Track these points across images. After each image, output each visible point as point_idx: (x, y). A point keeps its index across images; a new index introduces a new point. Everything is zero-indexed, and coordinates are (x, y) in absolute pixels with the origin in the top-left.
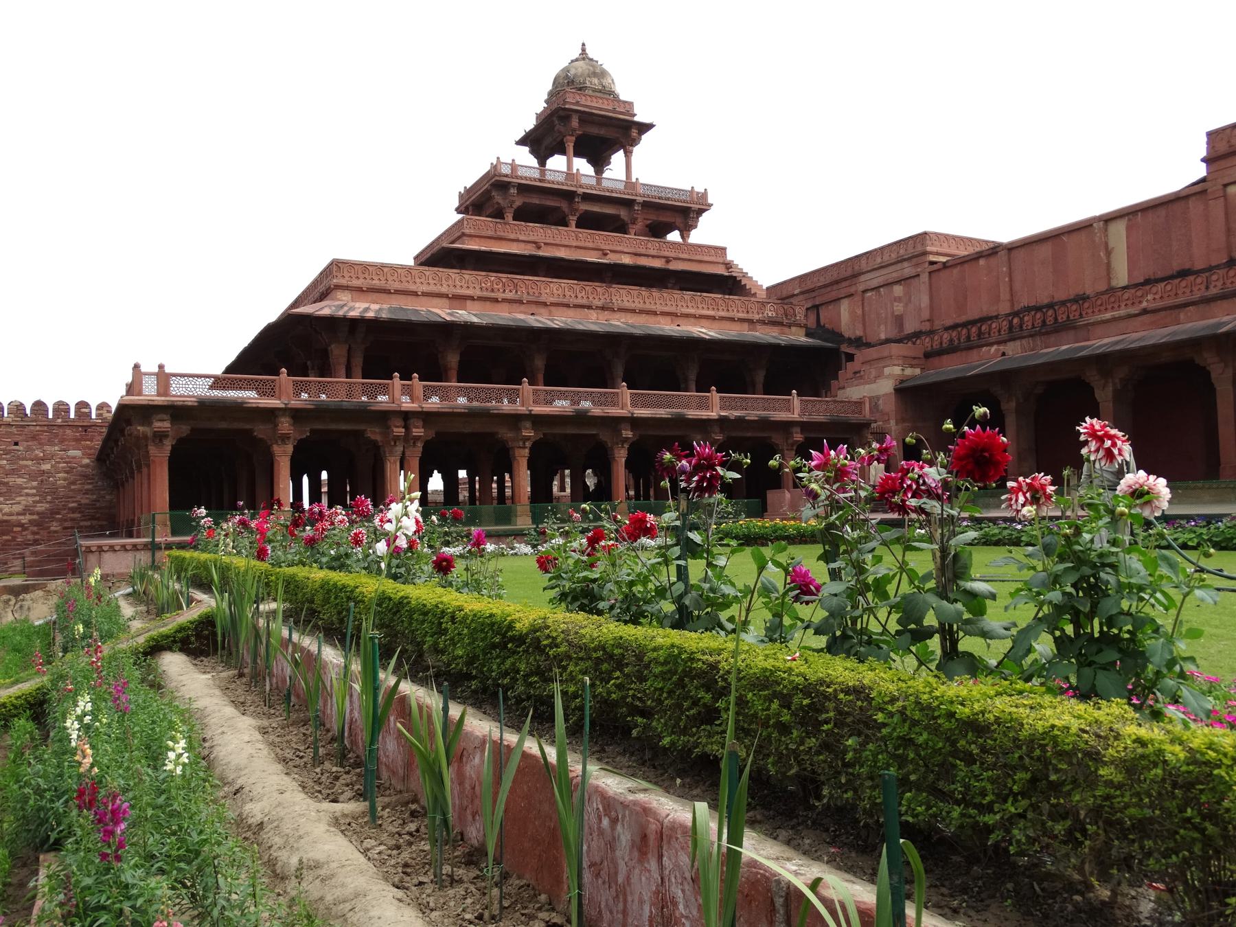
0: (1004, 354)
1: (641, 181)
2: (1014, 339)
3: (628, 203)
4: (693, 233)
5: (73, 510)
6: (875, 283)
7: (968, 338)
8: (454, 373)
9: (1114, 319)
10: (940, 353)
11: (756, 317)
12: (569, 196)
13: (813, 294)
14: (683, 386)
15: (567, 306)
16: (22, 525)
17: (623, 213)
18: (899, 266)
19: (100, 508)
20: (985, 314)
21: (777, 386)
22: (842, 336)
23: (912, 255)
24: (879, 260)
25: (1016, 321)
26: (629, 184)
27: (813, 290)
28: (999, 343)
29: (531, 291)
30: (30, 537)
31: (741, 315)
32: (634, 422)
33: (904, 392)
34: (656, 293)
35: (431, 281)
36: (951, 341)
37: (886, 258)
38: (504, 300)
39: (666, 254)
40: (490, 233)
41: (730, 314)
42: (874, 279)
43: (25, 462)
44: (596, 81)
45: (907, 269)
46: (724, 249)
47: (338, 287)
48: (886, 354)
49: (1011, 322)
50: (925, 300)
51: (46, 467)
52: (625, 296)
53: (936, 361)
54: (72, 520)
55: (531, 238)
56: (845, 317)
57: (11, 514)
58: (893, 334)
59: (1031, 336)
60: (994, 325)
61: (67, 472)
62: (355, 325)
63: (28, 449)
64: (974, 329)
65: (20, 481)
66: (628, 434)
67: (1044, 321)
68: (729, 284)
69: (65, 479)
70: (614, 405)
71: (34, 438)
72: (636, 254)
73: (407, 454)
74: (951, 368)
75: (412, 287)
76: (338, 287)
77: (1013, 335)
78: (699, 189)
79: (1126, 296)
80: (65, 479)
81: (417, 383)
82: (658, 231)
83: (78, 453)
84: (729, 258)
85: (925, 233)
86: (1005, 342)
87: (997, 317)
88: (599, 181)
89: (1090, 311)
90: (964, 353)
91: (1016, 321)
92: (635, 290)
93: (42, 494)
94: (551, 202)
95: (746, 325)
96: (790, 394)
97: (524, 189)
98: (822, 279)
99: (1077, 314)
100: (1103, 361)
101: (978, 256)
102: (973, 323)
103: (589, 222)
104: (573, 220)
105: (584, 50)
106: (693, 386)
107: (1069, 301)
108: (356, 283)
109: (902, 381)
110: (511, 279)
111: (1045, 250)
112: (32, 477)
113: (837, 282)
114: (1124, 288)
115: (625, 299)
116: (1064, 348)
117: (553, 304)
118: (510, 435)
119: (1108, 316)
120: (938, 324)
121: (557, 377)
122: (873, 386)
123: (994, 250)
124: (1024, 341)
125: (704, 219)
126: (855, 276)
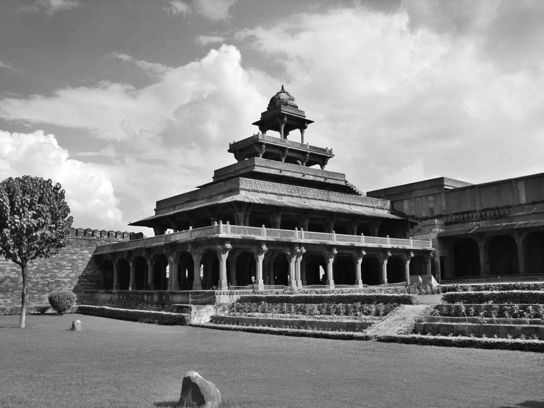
1: (309, 144)
2: (482, 220)
3: (304, 153)
4: (326, 166)
6: (421, 195)
7: (463, 218)
8: (279, 226)
9: (522, 215)
10: (451, 223)
11: (376, 206)
12: (283, 149)
15: (316, 200)
16: (64, 283)
19: (95, 277)
21: (382, 234)
22: (404, 214)
24: (422, 186)
25: (483, 213)
26: (302, 145)
28: (476, 221)
30: (68, 288)
32: (366, 249)
36: (456, 219)
38: (296, 197)
39: (325, 176)
40: (264, 165)
43: (67, 255)
44: (291, 102)
47: (242, 189)
48: (433, 223)
50: (444, 204)
51: (75, 257)
52: (334, 196)
53: (449, 226)
54: (84, 281)
56: (406, 207)
57: (60, 278)
59: (490, 219)
60: (474, 214)
61: (82, 260)
62: (250, 205)
63: (68, 249)
64: (466, 216)
65: (65, 263)
68: (347, 190)
69: (81, 263)
70: (360, 242)
71: (71, 244)
72: (315, 176)
74: (457, 230)
75: (266, 190)
76: (242, 189)
77: (482, 218)
78: (329, 149)
80: (81, 263)
81: (229, 226)
84: (347, 179)
86: (478, 221)
91: (483, 213)
92: (337, 194)
93: (73, 270)
94: (276, 151)
97: (268, 145)
100: (520, 230)
102: (466, 213)
103: (290, 160)
105: (283, 88)
106: (356, 233)
108: (247, 188)
109: (439, 234)
113: (403, 193)
114: (526, 204)
116: (504, 224)
117: (311, 199)
118: (327, 253)
119: (520, 214)
120: (448, 213)
121: (311, 228)
122: (428, 235)
125: (330, 161)
126: (411, 191)
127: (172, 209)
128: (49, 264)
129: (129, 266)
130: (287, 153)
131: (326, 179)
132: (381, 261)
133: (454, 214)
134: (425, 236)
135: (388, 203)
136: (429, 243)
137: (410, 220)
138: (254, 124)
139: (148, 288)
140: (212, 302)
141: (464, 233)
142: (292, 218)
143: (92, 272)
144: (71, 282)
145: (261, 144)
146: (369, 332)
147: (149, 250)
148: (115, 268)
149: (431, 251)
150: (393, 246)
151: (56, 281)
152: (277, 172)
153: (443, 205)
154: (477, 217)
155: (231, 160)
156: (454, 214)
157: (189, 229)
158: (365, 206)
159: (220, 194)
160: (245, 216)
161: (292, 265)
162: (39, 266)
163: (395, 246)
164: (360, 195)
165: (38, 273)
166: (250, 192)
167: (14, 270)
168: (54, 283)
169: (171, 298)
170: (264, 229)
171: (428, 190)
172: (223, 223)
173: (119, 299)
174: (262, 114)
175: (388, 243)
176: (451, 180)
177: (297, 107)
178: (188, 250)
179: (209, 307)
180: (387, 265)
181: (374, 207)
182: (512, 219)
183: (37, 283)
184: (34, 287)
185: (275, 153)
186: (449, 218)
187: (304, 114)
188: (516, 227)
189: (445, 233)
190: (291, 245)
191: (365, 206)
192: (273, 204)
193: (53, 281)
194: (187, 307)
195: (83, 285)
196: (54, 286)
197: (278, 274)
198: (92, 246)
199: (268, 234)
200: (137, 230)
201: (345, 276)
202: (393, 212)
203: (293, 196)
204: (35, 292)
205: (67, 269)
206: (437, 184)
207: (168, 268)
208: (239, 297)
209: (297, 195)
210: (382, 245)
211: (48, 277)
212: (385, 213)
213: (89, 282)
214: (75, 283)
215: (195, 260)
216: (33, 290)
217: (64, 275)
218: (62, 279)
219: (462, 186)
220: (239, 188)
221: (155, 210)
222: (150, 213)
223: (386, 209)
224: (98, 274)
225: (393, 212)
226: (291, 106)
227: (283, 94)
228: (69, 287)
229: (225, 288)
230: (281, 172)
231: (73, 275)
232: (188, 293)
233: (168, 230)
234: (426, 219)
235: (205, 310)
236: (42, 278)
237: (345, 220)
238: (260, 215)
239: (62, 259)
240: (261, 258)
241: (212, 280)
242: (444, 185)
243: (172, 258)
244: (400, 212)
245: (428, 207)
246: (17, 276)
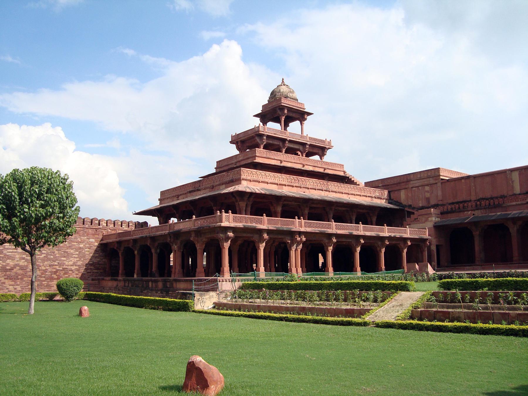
0: (474, 215)
1: (309, 136)
3: (304, 145)
4: (325, 156)
6: (417, 185)
7: (459, 208)
8: (279, 215)
9: (517, 205)
10: (447, 213)
11: (373, 196)
12: (284, 140)
15: (315, 189)
16: (72, 270)
18: (428, 179)
21: (380, 223)
24: (419, 176)
26: (302, 136)
28: (472, 210)
30: (75, 276)
31: (369, 195)
32: (364, 237)
34: (342, 185)
36: (452, 208)
37: (422, 175)
38: (296, 186)
40: (265, 156)
41: (365, 194)
44: (291, 95)
45: (432, 181)
47: (243, 179)
50: (440, 193)
51: (82, 246)
52: (333, 186)
54: (91, 269)
56: (403, 196)
58: (425, 204)
59: (485, 209)
60: (469, 204)
62: (251, 194)
63: (76, 238)
64: (461, 205)
65: (72, 251)
67: (489, 204)
68: (345, 180)
70: (358, 230)
71: (78, 233)
74: (453, 219)
75: (267, 180)
76: (243, 179)
77: (477, 208)
78: (328, 140)
79: (520, 197)
81: (231, 215)
83: (93, 240)
84: (345, 170)
85: (439, 168)
86: (474, 210)
87: (471, 201)
91: (478, 203)
93: (80, 258)
94: (276, 142)
97: (269, 137)
100: (514, 220)
101: (462, 178)
102: (461, 202)
103: (290, 151)
106: (354, 221)
108: (249, 178)
109: (435, 223)
112: (76, 250)
113: (400, 183)
114: (520, 194)
116: (499, 213)
117: (311, 189)
119: (514, 203)
120: (445, 202)
121: (311, 217)
122: (424, 224)
123: (468, 177)
125: (328, 152)
126: (408, 181)
127: (176, 198)
128: (56, 252)
129: (134, 255)
130: (287, 144)
131: (325, 169)
132: (378, 249)
135: (386, 192)
136: (425, 232)
137: (407, 209)
139: (152, 275)
140: (214, 289)
141: (460, 222)
142: (292, 207)
144: (78, 270)
145: (261, 136)
146: (367, 318)
147: (153, 239)
148: (120, 256)
150: (390, 234)
151: (64, 269)
152: (278, 163)
155: (233, 151)
156: (450, 204)
157: (192, 218)
159: (222, 184)
160: (246, 205)
161: (293, 253)
162: (47, 254)
163: (393, 235)
164: (359, 185)
165: (47, 261)
166: (252, 182)
167: (24, 258)
168: (61, 270)
169: (174, 285)
170: (265, 218)
171: (424, 180)
172: (226, 212)
173: (125, 286)
174: (263, 106)
175: (386, 231)
176: (447, 170)
177: (297, 100)
178: (192, 239)
179: (212, 293)
181: (372, 197)
182: (506, 208)
183: (46, 271)
184: (42, 274)
185: (275, 144)
187: (304, 106)
188: (509, 216)
189: (441, 222)
190: (292, 234)
192: (273, 193)
193: (61, 268)
194: (191, 294)
195: (90, 272)
197: (279, 261)
199: (269, 222)
200: (142, 219)
201: (343, 263)
202: (390, 201)
203: (293, 186)
204: (44, 279)
205: (75, 257)
206: (434, 174)
207: (172, 256)
208: (241, 283)
209: (297, 185)
210: (379, 233)
211: (56, 265)
212: (382, 203)
214: (82, 270)
215: (198, 248)
216: (42, 277)
217: (71, 263)
218: (70, 267)
219: (458, 176)
220: (240, 178)
221: (159, 200)
222: (154, 203)
223: (383, 199)
225: (390, 201)
226: (291, 98)
227: (283, 87)
228: (77, 274)
229: (227, 276)
230: (281, 162)
231: (80, 263)
232: (191, 281)
233: (172, 219)
234: (422, 208)
235: (208, 296)
236: (50, 266)
237: (344, 209)
238: (262, 204)
239: (70, 247)
240: (262, 247)
241: (215, 268)
242: (440, 175)
243: (176, 247)
244: (397, 202)
245: (425, 196)
246: (26, 264)
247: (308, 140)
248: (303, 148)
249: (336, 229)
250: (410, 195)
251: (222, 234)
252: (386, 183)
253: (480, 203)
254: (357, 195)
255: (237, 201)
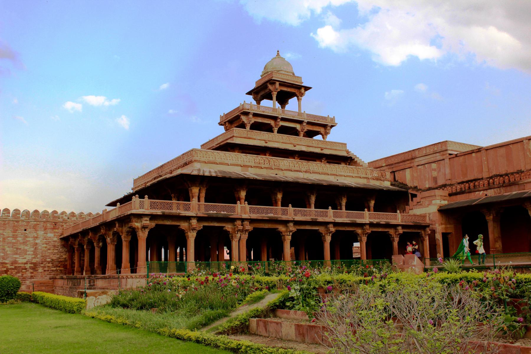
0: (486, 195)
2: (491, 189)
4: (328, 136)
5: (49, 262)
6: (423, 162)
7: (469, 187)
10: (456, 194)
13: (392, 166)
14: (339, 208)
16: (26, 269)
17: (298, 127)
20: (476, 177)
22: (406, 185)
23: (440, 151)
24: (424, 152)
26: (299, 114)
27: (392, 165)
28: (483, 190)
29: (276, 164)
33: (443, 211)
35: (234, 159)
36: (461, 189)
37: (428, 151)
40: (245, 136)
42: (423, 160)
43: (27, 239)
45: (438, 157)
46: (346, 144)
47: (195, 161)
48: (433, 194)
49: (489, 181)
50: (448, 171)
53: (454, 197)
54: (49, 267)
55: (263, 138)
56: (408, 178)
57: (22, 263)
58: (432, 185)
60: (481, 182)
61: (46, 244)
64: (472, 184)
66: (332, 229)
70: (327, 216)
73: (242, 237)
75: (226, 162)
76: (195, 161)
78: (331, 116)
80: (46, 247)
82: (310, 134)
84: (348, 148)
86: (487, 190)
87: (482, 179)
88: (283, 112)
89: (525, 177)
90: (467, 194)
91: (491, 181)
95: (366, 180)
96: (396, 212)
98: (396, 160)
99: (519, 178)
101: (472, 152)
102: (471, 181)
103: (283, 130)
104: (302, 134)
107: (515, 173)
108: (203, 159)
109: (440, 207)
110: (267, 158)
111: (503, 151)
113: (404, 161)
115: (315, 168)
116: (514, 193)
120: (454, 182)
122: (427, 209)
123: (479, 150)
124: (495, 190)
133: (459, 183)
134: (424, 209)
138: (247, 94)
142: (297, 193)
143: (58, 256)
149: (428, 226)
153: (447, 173)
154: (484, 185)
156: (459, 183)
158: (356, 177)
160: (200, 190)
168: (13, 269)
174: (256, 82)
180: (366, 243)
186: (454, 187)
189: (448, 205)
191: (356, 177)
193: (13, 267)
195: (48, 271)
196: (14, 272)
198: (58, 229)
199: (152, 207)
209: (266, 166)
213: (54, 267)
217: (24, 261)
224: (65, 259)
245: (432, 176)
247: (306, 117)
248: (325, 129)
249: (295, 215)
250: (415, 175)
251: (137, 222)
252: (390, 162)
253: (493, 180)
254: (347, 176)
255: (189, 187)
